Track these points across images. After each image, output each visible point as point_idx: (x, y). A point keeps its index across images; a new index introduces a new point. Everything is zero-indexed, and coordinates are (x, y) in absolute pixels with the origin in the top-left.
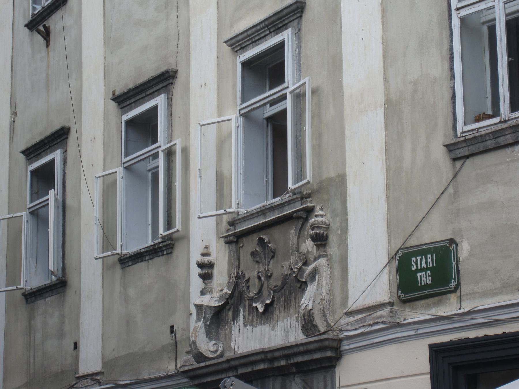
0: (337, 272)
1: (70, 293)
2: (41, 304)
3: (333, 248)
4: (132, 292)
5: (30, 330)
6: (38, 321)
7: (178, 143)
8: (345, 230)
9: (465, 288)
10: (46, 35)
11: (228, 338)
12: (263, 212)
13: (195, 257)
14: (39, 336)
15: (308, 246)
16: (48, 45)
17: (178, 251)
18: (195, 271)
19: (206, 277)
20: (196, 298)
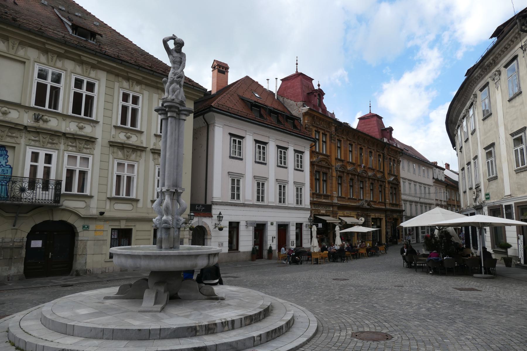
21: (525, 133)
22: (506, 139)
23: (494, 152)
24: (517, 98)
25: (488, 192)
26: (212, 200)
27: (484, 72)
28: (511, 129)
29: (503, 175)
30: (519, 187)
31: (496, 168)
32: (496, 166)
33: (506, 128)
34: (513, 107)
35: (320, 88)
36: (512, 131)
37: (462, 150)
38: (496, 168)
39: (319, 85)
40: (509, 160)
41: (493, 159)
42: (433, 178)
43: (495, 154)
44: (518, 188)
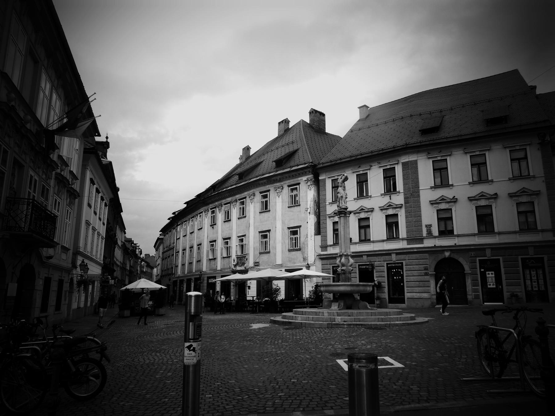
0: (248, 263)
1: (216, 260)
2: (212, 261)
3: (248, 260)
4: (224, 261)
5: (210, 263)
6: (211, 263)
7: (231, 246)
8: (249, 259)
9: (260, 266)
10: (213, 228)
11: (236, 268)
12: (241, 255)
13: (233, 259)
14: (211, 264)
15: (245, 260)
16: (213, 228)
17: (231, 258)
18: (233, 260)
19: (234, 261)
20: (233, 263)
21: (300, 229)
22: (283, 229)
23: (269, 235)
24: (296, 207)
25: (257, 261)
26: (78, 250)
27: (268, 182)
28: (287, 224)
29: (276, 251)
30: (290, 260)
31: (269, 246)
32: (269, 245)
33: (283, 223)
34: (291, 211)
35: (108, 140)
36: (289, 226)
37: (215, 226)
38: (269, 246)
39: (107, 138)
40: (283, 243)
41: (268, 240)
42: (122, 242)
43: (269, 237)
44: (289, 260)
